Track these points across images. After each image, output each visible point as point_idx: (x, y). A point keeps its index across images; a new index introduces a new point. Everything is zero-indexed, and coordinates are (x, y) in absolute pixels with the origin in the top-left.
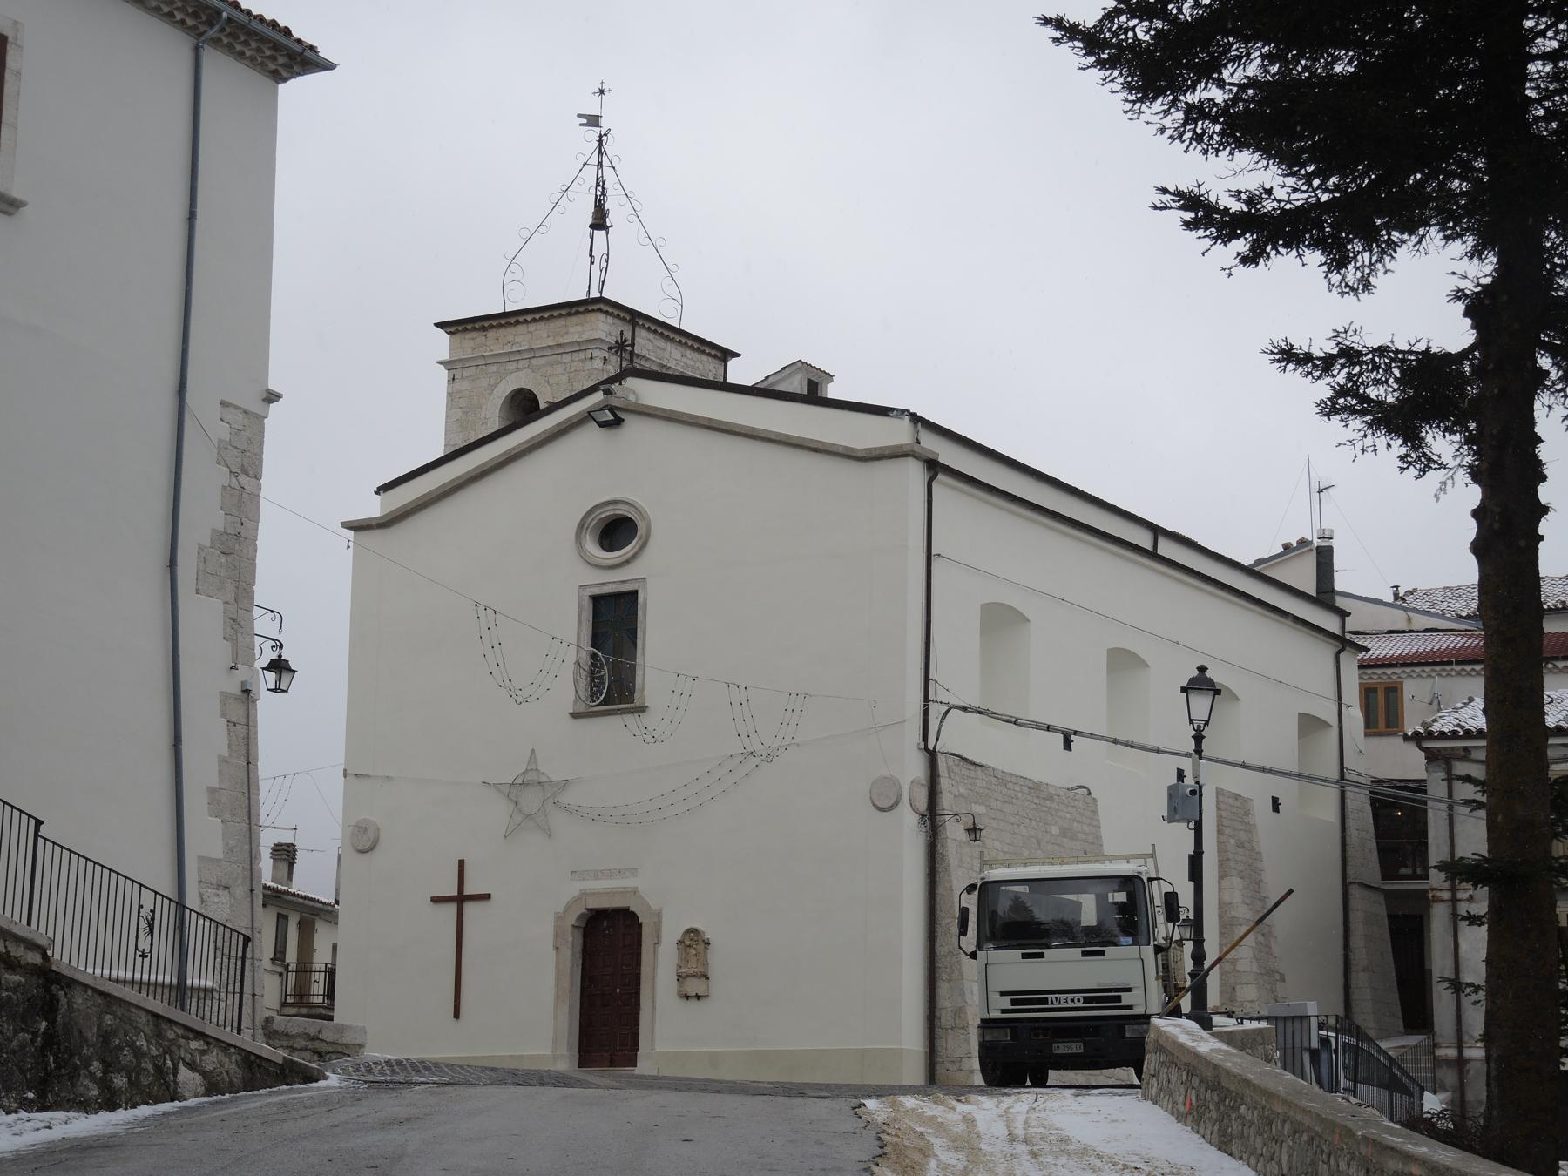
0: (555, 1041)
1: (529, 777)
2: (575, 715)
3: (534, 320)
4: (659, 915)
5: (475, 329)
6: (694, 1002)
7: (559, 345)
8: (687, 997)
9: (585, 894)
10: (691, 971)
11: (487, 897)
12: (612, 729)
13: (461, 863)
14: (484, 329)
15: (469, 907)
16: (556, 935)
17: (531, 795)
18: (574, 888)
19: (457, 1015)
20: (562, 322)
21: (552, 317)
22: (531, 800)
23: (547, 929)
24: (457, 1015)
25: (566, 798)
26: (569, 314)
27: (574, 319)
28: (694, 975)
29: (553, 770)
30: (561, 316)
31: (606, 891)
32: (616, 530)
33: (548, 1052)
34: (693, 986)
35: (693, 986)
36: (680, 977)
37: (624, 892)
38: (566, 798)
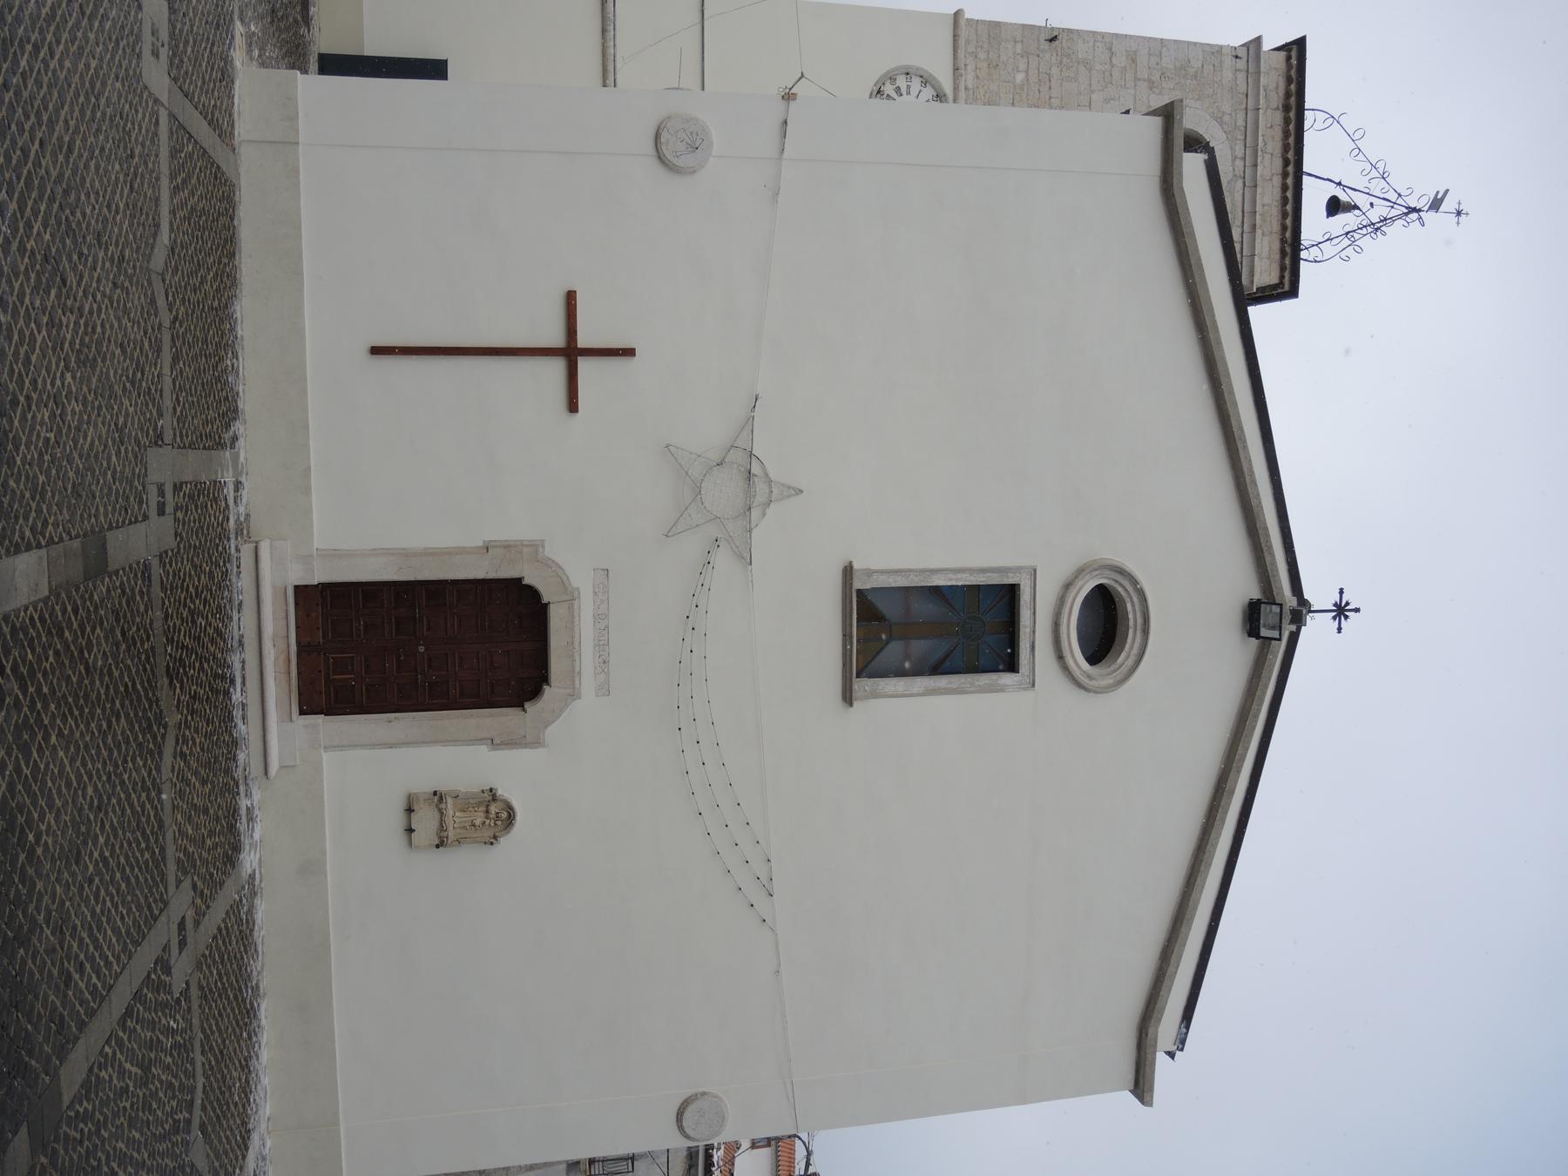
0: (335, 555)
1: (760, 487)
2: (848, 571)
3: (1284, 188)
4: (537, 743)
5: (1288, 95)
6: (399, 820)
7: (1254, 227)
8: (410, 810)
9: (572, 597)
10: (449, 822)
11: (573, 406)
12: (822, 633)
13: (629, 352)
14: (1286, 108)
15: (557, 367)
16: (507, 546)
17: (733, 488)
18: (581, 578)
19: (376, 351)
20: (1276, 227)
21: (1284, 215)
22: (723, 492)
23: (519, 530)
24: (376, 351)
25: (723, 558)
26: (1283, 241)
27: (1277, 246)
28: (442, 827)
29: (767, 533)
30: (1284, 228)
31: (575, 639)
32: (1107, 624)
33: (317, 543)
34: (426, 821)
35: (426, 821)
36: (438, 797)
37: (573, 675)
38: (723, 558)
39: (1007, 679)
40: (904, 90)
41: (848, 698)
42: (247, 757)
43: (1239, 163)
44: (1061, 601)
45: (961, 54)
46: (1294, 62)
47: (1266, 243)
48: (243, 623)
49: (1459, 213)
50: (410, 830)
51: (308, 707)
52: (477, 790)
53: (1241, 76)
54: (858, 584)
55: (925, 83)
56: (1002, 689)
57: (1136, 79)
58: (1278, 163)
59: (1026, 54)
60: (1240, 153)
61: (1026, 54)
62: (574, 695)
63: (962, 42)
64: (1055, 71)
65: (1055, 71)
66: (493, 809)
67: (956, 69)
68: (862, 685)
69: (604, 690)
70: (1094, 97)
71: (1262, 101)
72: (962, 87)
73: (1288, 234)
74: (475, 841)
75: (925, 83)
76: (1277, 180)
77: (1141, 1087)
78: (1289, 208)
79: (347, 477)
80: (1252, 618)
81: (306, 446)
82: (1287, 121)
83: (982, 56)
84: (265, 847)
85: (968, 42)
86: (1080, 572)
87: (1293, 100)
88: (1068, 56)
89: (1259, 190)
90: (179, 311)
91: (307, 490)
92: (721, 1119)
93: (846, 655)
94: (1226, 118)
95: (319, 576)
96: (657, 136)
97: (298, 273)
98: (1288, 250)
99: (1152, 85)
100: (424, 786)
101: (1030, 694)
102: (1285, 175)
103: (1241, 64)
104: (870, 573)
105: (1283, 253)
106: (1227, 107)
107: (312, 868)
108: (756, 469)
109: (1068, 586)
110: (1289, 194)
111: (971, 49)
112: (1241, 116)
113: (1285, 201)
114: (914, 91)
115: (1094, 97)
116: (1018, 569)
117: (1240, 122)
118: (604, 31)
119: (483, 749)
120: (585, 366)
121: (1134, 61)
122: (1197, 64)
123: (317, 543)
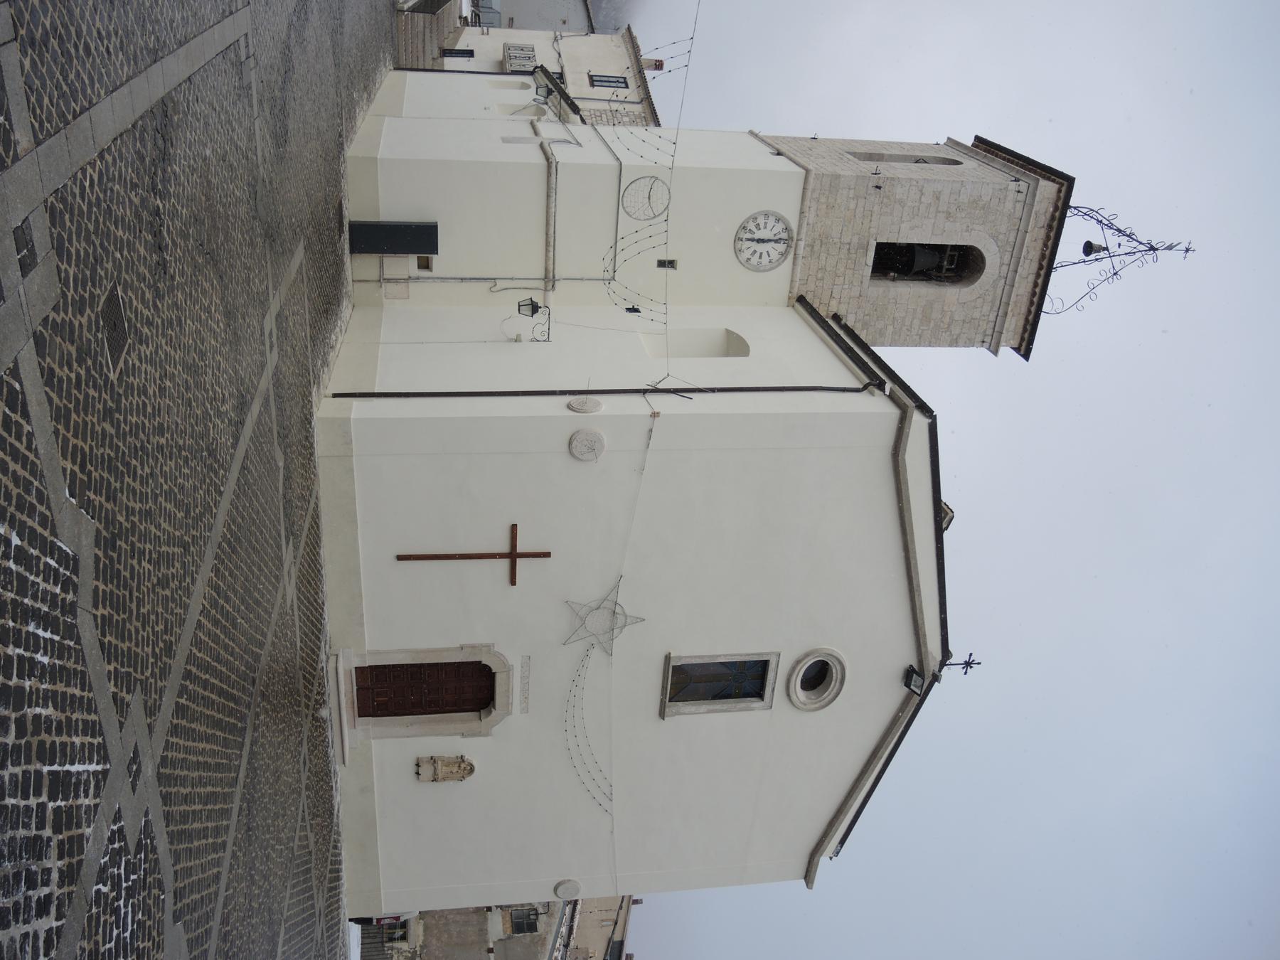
0: (377, 653)
1: (620, 620)
2: (668, 658)
3: (1036, 285)
4: (487, 735)
5: (1053, 218)
6: (413, 769)
7: (1006, 314)
8: (418, 765)
9: (508, 670)
10: (439, 771)
11: (513, 582)
12: (651, 683)
13: (547, 555)
14: (1050, 227)
15: (505, 563)
16: (473, 647)
17: (604, 620)
18: (514, 660)
19: (400, 558)
20: (1024, 310)
21: (1032, 303)
22: (598, 622)
23: (479, 638)
24: (400, 558)
25: (596, 653)
26: (1027, 320)
27: (1021, 323)
28: (435, 770)
29: (621, 642)
30: (1029, 312)
31: (509, 689)
32: (819, 676)
33: (368, 647)
34: (426, 770)
35: (426, 770)
36: (433, 760)
37: (508, 705)
38: (596, 653)
39: (755, 703)
40: (762, 226)
41: (662, 715)
42: (334, 752)
43: (1005, 268)
44: (793, 669)
45: (807, 203)
46: (1062, 195)
47: (1014, 321)
48: (330, 687)
49: (1187, 250)
50: (418, 773)
51: (362, 714)
52: (453, 756)
53: (1019, 206)
54: (673, 663)
55: (778, 220)
56: (752, 709)
57: (938, 212)
58: (1035, 266)
59: (857, 197)
60: (1006, 260)
61: (857, 197)
62: (509, 713)
63: (809, 194)
64: (876, 208)
65: (876, 208)
66: (463, 766)
67: (802, 212)
68: (672, 707)
69: (525, 710)
70: (903, 226)
71: (1024, 253)
72: (805, 225)
73: (1031, 318)
74: (452, 779)
75: (778, 220)
76: (1031, 278)
77: (809, 876)
78: (1035, 300)
79: (384, 618)
80: (908, 675)
81: (361, 604)
82: (1048, 237)
83: (823, 200)
84: (344, 781)
85: (814, 190)
86: (807, 655)
87: (1055, 224)
88: (888, 197)
89: (1008, 320)
90: (283, 505)
91: (362, 625)
92: (578, 891)
93: (664, 688)
94: (1001, 237)
95: (369, 662)
96: (570, 443)
97: (355, 522)
98: (1029, 327)
99: (948, 215)
100: (426, 754)
101: (769, 712)
102: (1038, 275)
103: (1021, 197)
104: (680, 658)
105: (1025, 330)
106: (1003, 229)
107: (367, 790)
108: (618, 610)
109: (798, 662)
110: (1038, 290)
111: (816, 195)
112: (1013, 235)
113: (1034, 294)
114: (769, 226)
115: (903, 226)
116: (767, 654)
117: (1012, 239)
118: (548, 196)
119: (458, 738)
120: (520, 549)
121: (938, 198)
122: (986, 199)
123: (368, 647)
